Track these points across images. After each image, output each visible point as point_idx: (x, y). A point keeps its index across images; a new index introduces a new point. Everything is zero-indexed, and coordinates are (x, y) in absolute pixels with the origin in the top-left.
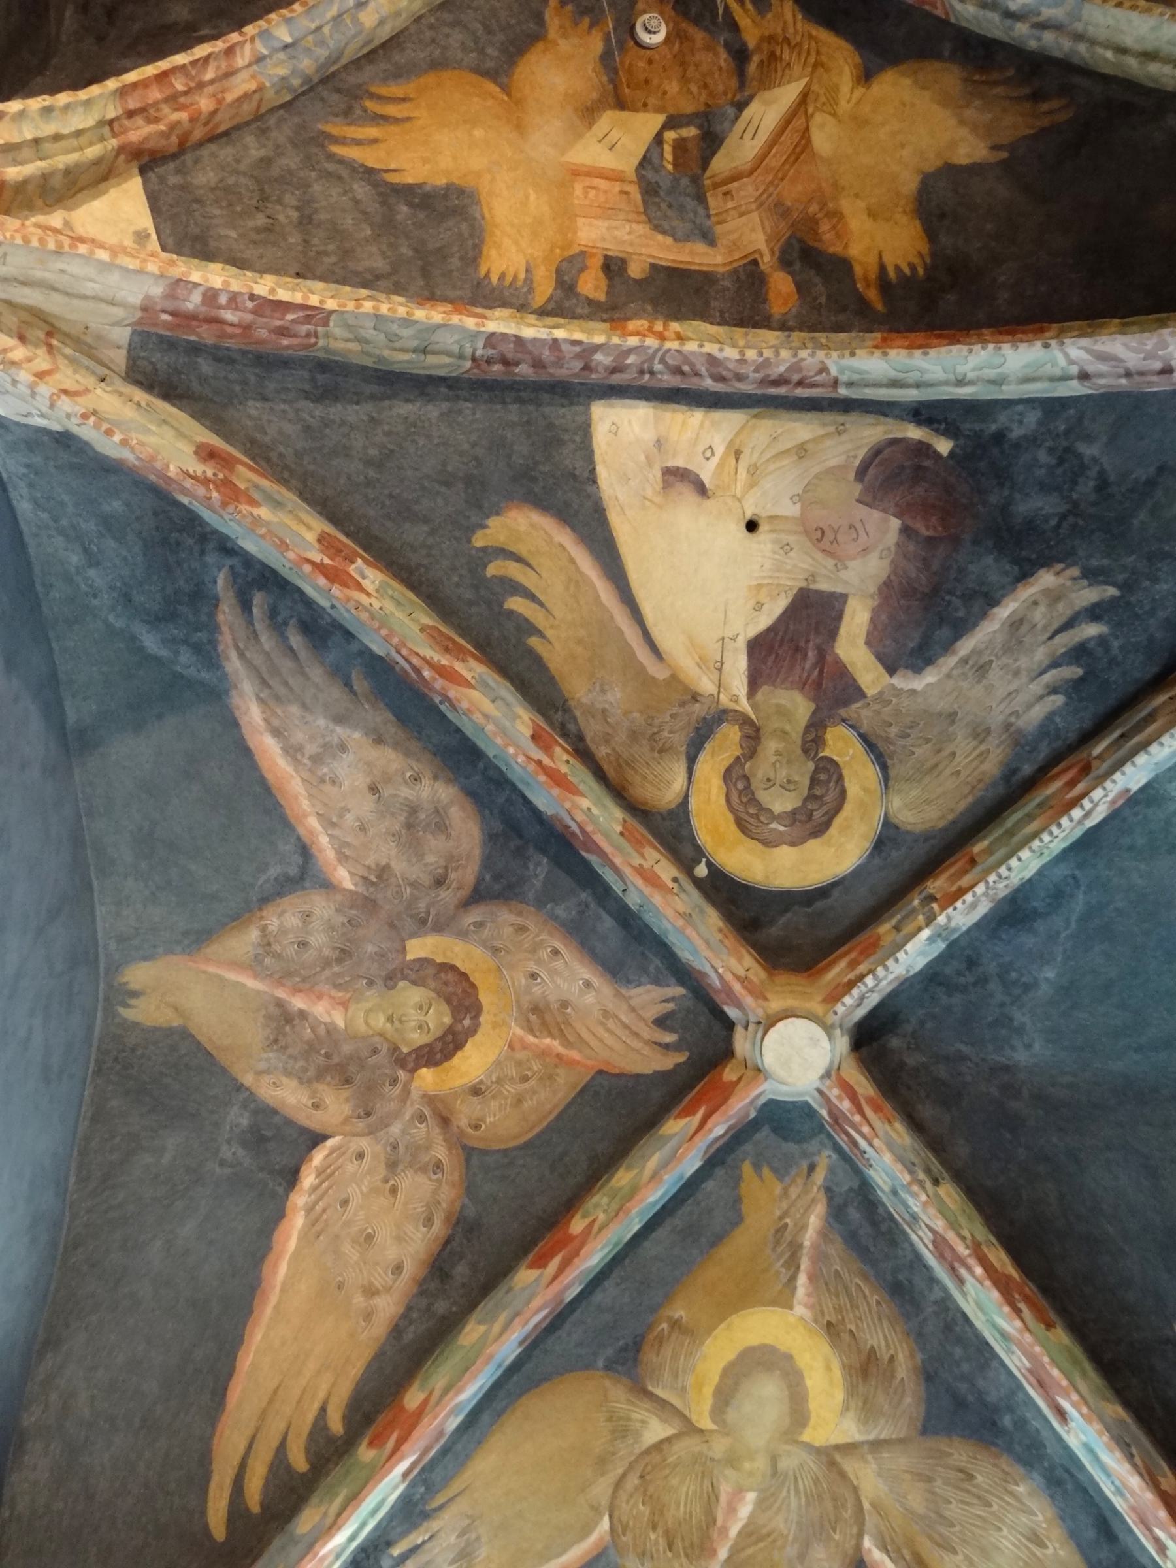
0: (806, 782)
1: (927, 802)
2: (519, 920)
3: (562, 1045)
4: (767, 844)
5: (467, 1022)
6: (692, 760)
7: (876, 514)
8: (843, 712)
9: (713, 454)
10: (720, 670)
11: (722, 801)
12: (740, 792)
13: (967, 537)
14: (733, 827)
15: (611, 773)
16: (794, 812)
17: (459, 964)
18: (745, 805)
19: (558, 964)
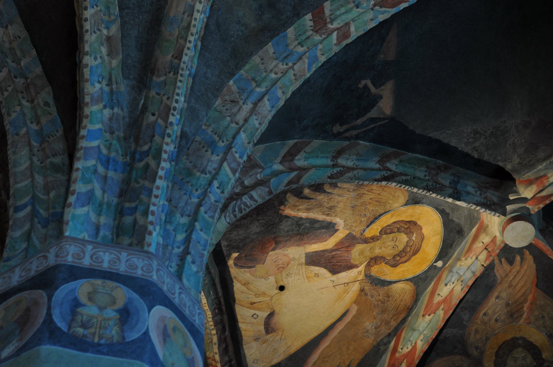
0: (392, 235)
1: (394, 196)
2: (473, 333)
3: (526, 303)
4: (423, 239)
5: (520, 342)
6: (391, 283)
7: (268, 258)
8: (358, 236)
9: (255, 314)
10: (348, 283)
11: (407, 264)
12: (401, 257)
13: (273, 236)
14: (418, 255)
15: (402, 316)
16: (406, 234)
17: (495, 351)
18: (406, 253)
19: (490, 312)
